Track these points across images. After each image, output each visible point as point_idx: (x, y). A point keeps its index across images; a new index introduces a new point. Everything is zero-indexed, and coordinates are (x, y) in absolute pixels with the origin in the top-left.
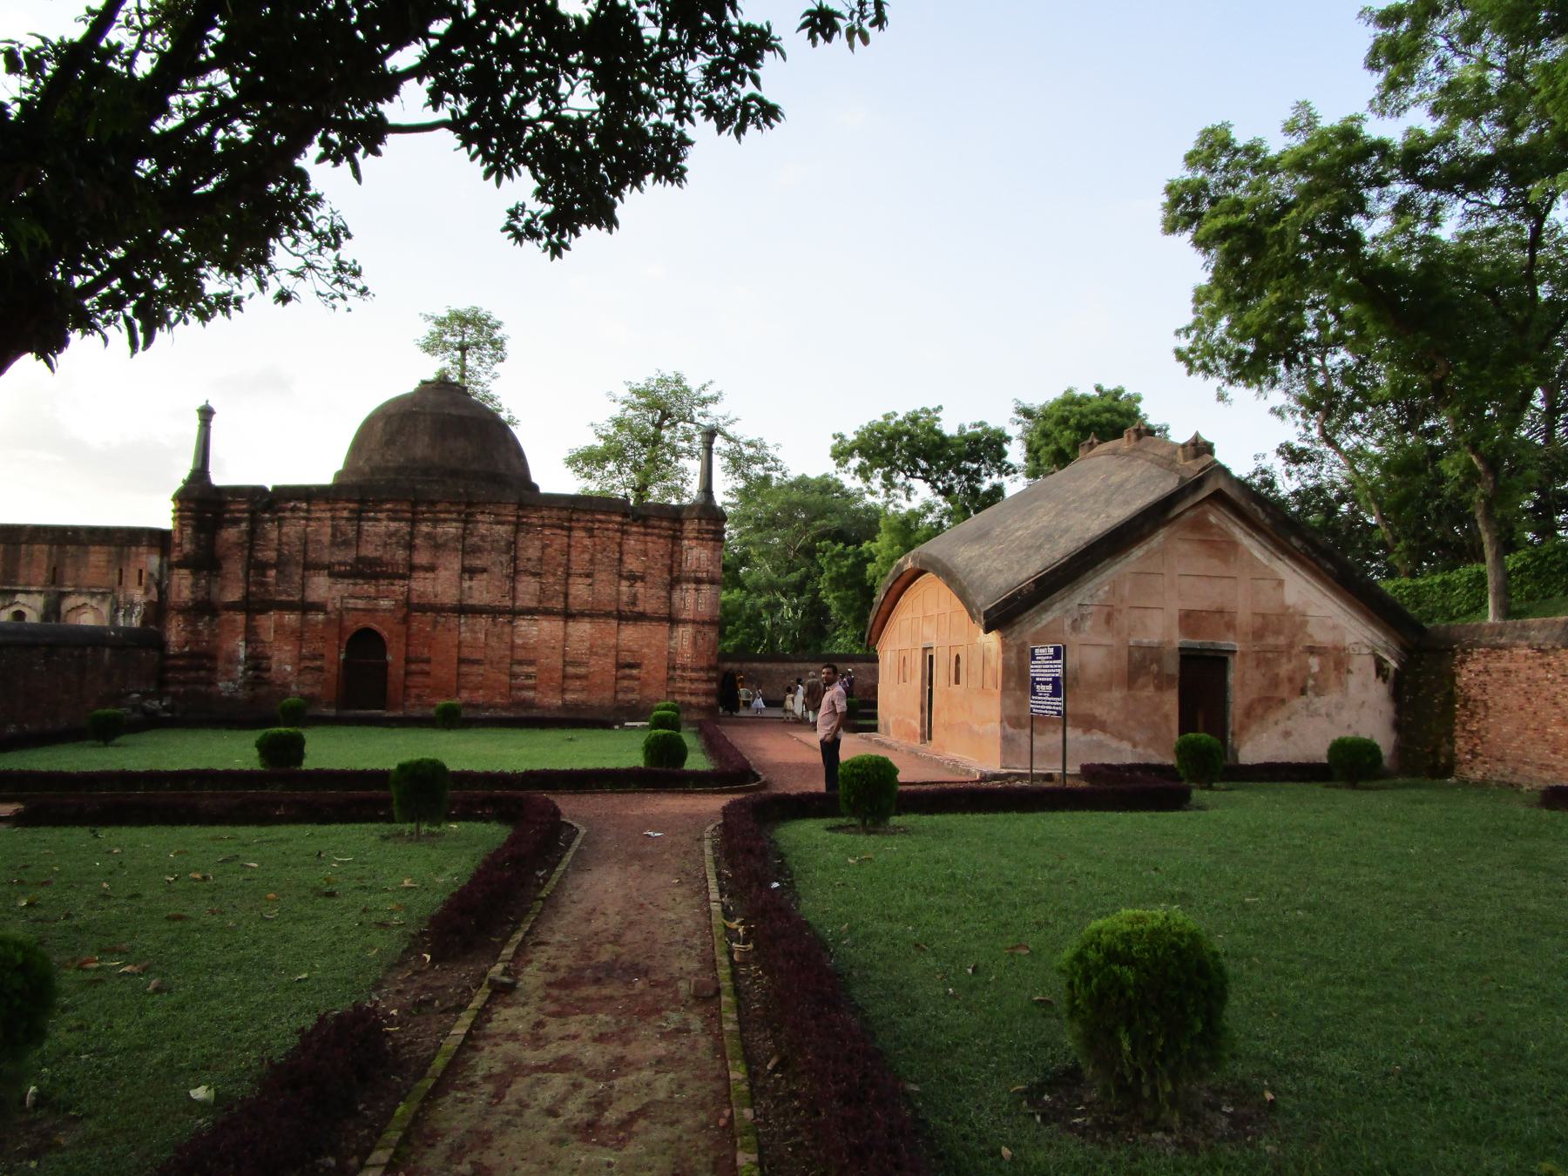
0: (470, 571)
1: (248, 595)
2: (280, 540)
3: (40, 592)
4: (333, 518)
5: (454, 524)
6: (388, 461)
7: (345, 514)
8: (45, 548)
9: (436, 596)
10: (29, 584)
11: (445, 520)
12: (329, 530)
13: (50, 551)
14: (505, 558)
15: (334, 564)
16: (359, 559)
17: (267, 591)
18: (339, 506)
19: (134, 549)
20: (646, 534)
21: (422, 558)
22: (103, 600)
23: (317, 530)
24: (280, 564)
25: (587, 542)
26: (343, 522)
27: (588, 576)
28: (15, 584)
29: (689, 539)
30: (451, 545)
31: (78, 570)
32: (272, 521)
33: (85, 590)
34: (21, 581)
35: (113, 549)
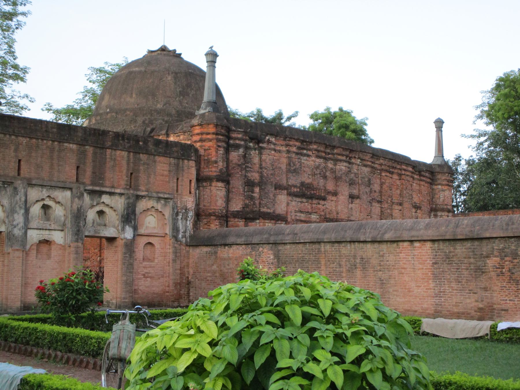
0: (352, 197)
1: (243, 208)
2: (261, 165)
3: (121, 194)
4: (288, 152)
5: (345, 164)
6: (185, 108)
7: (294, 149)
8: (125, 154)
9: (338, 214)
10: (113, 187)
11: (341, 161)
12: (285, 161)
13: (128, 157)
14: (368, 190)
15: (291, 186)
16: (303, 184)
17: (254, 204)
18: (291, 143)
19: (186, 161)
20: (421, 180)
21: (330, 186)
22: (165, 205)
23: (278, 160)
24: (261, 184)
25: (398, 182)
26: (293, 155)
27: (401, 204)
28: (102, 185)
29: (442, 185)
30: (344, 177)
31: (149, 177)
32: (255, 149)
33: (155, 195)
34: (107, 183)
35: (172, 161)
